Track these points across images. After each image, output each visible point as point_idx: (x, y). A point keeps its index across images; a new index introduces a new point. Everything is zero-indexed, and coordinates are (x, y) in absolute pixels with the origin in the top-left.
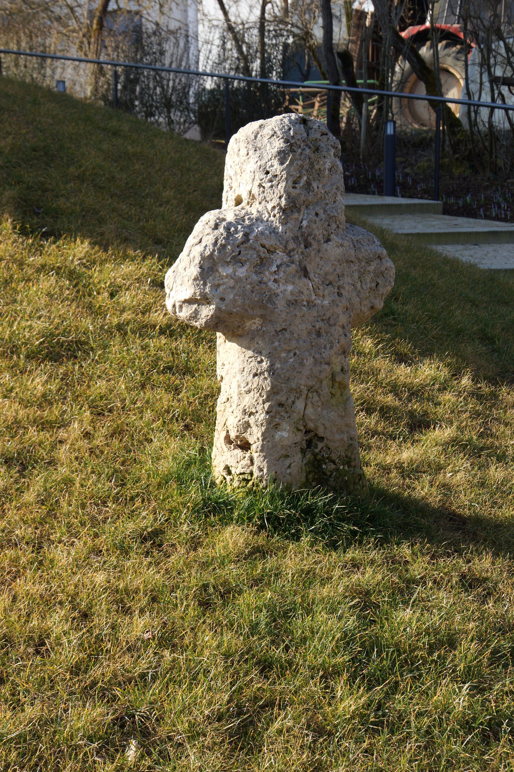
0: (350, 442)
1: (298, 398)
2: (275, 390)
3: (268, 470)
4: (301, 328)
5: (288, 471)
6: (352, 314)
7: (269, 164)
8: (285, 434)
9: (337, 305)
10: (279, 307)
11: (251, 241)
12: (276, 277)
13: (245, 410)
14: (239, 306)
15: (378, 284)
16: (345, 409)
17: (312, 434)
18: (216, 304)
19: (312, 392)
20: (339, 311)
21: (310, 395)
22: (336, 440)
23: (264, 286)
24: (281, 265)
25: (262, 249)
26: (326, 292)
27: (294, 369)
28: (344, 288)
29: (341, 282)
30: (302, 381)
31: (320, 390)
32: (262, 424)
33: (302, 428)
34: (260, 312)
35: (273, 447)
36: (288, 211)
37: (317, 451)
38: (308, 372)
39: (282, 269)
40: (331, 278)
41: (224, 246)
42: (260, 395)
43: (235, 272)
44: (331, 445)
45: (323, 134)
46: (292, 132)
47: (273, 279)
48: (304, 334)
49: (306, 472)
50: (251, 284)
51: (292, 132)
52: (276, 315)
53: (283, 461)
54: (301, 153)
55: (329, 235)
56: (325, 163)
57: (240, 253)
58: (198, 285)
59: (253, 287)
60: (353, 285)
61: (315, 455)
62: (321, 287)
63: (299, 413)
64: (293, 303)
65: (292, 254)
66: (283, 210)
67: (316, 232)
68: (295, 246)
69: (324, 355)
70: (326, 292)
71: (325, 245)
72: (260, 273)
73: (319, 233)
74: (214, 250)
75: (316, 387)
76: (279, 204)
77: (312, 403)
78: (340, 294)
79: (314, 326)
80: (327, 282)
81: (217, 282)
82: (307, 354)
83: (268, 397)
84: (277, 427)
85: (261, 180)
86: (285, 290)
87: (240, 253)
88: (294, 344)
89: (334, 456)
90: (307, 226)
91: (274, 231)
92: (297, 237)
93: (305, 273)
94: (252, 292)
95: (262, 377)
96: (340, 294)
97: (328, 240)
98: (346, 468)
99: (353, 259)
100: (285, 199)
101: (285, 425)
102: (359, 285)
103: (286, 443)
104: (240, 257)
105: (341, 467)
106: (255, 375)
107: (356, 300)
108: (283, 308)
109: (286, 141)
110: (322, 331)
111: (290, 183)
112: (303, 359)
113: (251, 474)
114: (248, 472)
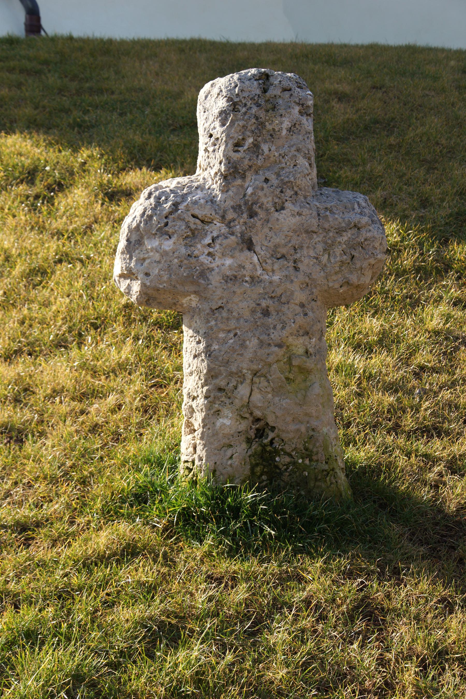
0: (311, 433)
1: (242, 383)
2: (213, 373)
3: (206, 460)
4: (242, 305)
5: (229, 462)
6: (314, 290)
7: (212, 126)
8: (227, 421)
9: (292, 281)
10: (213, 282)
11: (180, 211)
12: (211, 250)
13: (189, 393)
14: (165, 282)
15: (353, 257)
16: (305, 396)
17: (262, 423)
18: (141, 280)
19: (259, 377)
20: (295, 287)
21: (256, 380)
22: (289, 431)
23: (193, 260)
24: (218, 237)
25: (192, 220)
26: (276, 267)
27: (234, 350)
28: (302, 262)
29: (298, 255)
30: (244, 365)
31: (268, 375)
32: (202, 410)
33: (247, 415)
34: (192, 288)
35: (213, 435)
36: (229, 178)
37: (265, 441)
38: (251, 355)
39: (218, 241)
40: (283, 251)
41: (150, 217)
42: (199, 378)
43: (160, 245)
44: (284, 436)
45: (284, 90)
46: (237, 90)
47: (206, 252)
48: (247, 314)
49: (251, 464)
50: (178, 257)
51: (237, 90)
52: (211, 292)
53: (225, 451)
54: (245, 113)
55: (283, 203)
56: (281, 123)
57: (166, 224)
58: (125, 259)
59: (181, 261)
60: (317, 258)
61: (264, 447)
62: (269, 261)
63: (242, 399)
64: (232, 279)
65: (232, 224)
66: (225, 177)
67: (264, 200)
68: (234, 215)
69: (272, 336)
70: (276, 267)
71: (276, 214)
72: (191, 246)
73: (267, 201)
74: (140, 222)
75: (264, 371)
76: (219, 170)
77: (258, 388)
78: (296, 269)
79: (258, 305)
80: (279, 256)
81: (142, 256)
82: (250, 334)
83: (206, 381)
84: (218, 413)
85: (206, 144)
86: (223, 265)
87: (166, 224)
88: (233, 324)
89: (288, 449)
90: (252, 194)
91: (212, 200)
92: (240, 206)
93: (249, 245)
94: (180, 266)
95: (200, 358)
96: (296, 269)
97: (280, 208)
98: (307, 462)
99: (314, 229)
100: (225, 164)
101: (226, 412)
102: (324, 259)
103: (227, 431)
104: (166, 229)
105: (300, 461)
106: (195, 356)
107: (318, 275)
108: (218, 285)
109: (229, 99)
110: (271, 309)
111: (230, 145)
112: (244, 341)
113: (193, 462)
114: (190, 460)
